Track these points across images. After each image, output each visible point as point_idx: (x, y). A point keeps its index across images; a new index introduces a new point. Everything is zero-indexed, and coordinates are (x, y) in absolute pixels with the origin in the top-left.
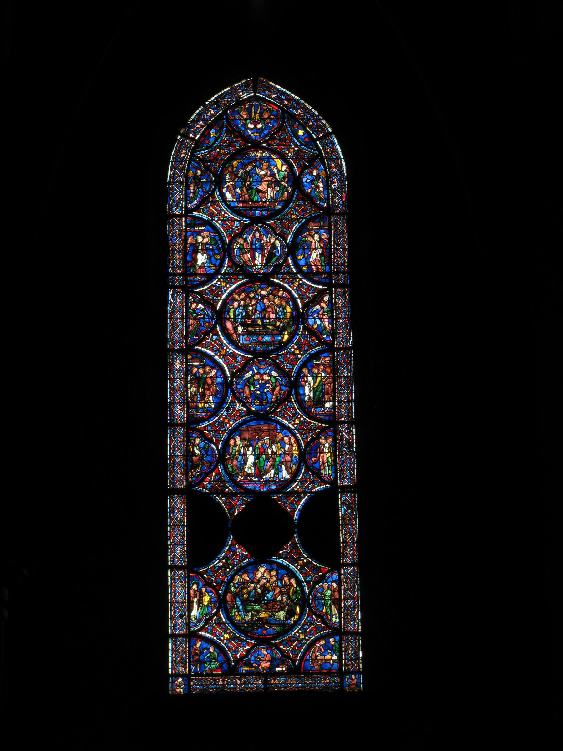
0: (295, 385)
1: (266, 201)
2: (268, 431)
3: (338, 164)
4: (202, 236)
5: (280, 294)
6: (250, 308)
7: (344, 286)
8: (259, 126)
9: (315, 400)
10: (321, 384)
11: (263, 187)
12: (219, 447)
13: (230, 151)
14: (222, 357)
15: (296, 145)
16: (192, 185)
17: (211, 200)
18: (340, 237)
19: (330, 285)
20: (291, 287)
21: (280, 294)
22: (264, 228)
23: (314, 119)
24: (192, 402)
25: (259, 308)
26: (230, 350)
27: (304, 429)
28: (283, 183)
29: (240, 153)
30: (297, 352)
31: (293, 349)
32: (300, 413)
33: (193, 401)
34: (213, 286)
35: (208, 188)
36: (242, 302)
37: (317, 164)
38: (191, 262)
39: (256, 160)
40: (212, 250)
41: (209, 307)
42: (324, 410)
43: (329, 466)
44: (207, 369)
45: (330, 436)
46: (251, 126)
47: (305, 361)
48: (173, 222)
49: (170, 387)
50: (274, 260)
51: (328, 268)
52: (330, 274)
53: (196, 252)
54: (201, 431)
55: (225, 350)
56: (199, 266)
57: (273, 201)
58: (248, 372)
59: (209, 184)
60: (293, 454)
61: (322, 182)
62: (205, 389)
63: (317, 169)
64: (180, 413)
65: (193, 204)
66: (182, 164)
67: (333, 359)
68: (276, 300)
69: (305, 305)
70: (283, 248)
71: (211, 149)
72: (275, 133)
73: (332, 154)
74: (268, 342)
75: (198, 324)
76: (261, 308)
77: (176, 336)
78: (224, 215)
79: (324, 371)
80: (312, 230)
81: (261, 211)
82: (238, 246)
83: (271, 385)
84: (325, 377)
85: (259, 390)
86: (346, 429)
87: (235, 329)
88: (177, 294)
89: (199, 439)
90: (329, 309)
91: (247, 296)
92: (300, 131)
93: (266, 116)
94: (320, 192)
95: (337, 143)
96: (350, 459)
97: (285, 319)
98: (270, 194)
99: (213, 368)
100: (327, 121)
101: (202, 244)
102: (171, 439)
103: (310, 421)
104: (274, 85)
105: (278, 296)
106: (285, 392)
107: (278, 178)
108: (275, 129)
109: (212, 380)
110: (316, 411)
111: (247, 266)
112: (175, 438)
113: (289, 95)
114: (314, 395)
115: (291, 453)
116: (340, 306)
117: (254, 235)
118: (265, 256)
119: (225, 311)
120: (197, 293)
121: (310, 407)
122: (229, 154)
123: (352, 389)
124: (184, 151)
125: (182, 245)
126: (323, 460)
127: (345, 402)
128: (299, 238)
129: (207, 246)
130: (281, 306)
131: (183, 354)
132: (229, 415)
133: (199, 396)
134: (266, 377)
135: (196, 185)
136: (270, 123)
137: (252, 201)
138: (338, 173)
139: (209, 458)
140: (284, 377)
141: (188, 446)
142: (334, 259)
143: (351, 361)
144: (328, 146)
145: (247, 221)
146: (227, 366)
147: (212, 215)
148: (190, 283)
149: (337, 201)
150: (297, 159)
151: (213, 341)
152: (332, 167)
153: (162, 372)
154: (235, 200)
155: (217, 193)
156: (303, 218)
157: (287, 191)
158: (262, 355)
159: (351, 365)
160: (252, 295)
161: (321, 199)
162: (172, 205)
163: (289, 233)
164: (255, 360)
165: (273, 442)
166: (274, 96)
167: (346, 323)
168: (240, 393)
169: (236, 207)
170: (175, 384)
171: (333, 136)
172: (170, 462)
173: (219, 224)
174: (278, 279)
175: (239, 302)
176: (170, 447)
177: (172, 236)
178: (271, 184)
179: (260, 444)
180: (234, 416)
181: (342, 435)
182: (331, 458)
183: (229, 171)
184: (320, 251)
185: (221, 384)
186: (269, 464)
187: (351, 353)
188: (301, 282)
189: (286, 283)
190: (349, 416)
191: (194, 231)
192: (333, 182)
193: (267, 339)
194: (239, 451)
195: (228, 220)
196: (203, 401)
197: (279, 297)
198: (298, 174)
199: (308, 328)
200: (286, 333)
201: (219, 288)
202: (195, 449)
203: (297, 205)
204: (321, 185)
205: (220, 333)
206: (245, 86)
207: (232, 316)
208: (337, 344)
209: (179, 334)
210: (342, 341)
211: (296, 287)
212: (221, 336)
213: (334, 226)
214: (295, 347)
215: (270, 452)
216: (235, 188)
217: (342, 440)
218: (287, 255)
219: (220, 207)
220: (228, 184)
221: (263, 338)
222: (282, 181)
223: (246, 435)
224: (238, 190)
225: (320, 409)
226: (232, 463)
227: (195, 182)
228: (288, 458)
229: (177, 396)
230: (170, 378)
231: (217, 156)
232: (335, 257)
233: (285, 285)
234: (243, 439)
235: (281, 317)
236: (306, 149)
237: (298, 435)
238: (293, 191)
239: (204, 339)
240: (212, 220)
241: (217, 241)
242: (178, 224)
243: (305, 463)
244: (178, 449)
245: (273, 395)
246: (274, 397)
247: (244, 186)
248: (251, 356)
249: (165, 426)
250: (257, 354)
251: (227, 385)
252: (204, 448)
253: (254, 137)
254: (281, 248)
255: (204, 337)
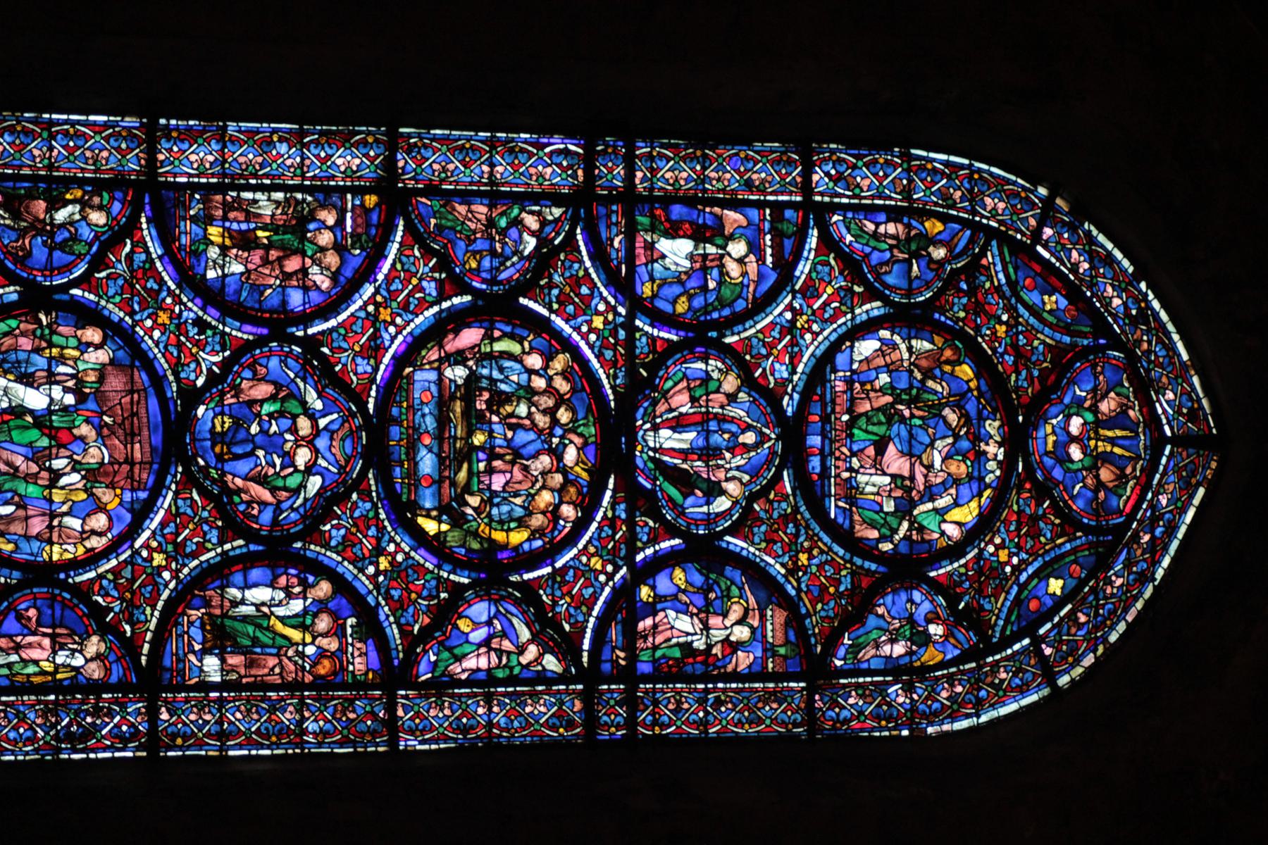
0: (278, 553)
1: (851, 470)
2: (126, 461)
3: (960, 706)
4: (746, 256)
5: (568, 511)
6: (522, 410)
7: (591, 720)
8: (1075, 452)
9: (228, 622)
10: (279, 641)
11: (895, 461)
12: (76, 292)
13: (1002, 355)
14: (371, 308)
15: (1017, 570)
16: (900, 227)
17: (857, 289)
18: (741, 712)
19: (591, 677)
20: (585, 547)
21: (568, 511)
22: (768, 462)
23: (1096, 628)
24: (224, 203)
25: (522, 437)
26: (393, 339)
27: (134, 580)
28: (905, 525)
29: (996, 390)
30: (384, 563)
31: (392, 548)
32: (186, 571)
33: (227, 207)
34: (593, 286)
35: (890, 280)
36: (539, 383)
37: (960, 636)
38: (668, 219)
39: (977, 437)
40: (704, 289)
41: (528, 270)
42: (194, 652)
43: (9, 666)
44: (332, 259)
45: (108, 671)
46: (1075, 425)
47: (355, 590)
48: (790, 162)
49: (275, 131)
50: (673, 492)
51: (645, 668)
52: (628, 675)
53: (699, 234)
54: (129, 229)
55: (393, 323)
56: (653, 243)
57: (851, 493)
58: (320, 397)
59: (904, 284)
60: (51, 543)
61: (910, 653)
62: (267, 248)
63: (946, 636)
64: (191, 160)
65: (844, 231)
66: (962, 199)
67: (360, 685)
68: (546, 498)
69: (529, 590)
70: (710, 520)
71: (1008, 293)
72: (1054, 504)
73: (992, 685)
74: (416, 464)
75: (474, 232)
76: (524, 446)
77: (437, 158)
78: (809, 330)
79: (322, 653)
80: (763, 618)
81: (822, 450)
82: (715, 375)
83: (277, 474)
84: (302, 655)
85: (264, 432)
86: (131, 725)
87: (459, 358)
88: (570, 167)
89: (102, 221)
90: (517, 670)
91: (560, 400)
92: (1060, 582)
93: (1106, 474)
94: (877, 647)
95: (1024, 702)
96: (32, 740)
97: (489, 524)
98: (871, 482)
99: (335, 277)
100: (1089, 670)
101: (722, 256)
102: (106, 126)
103: (160, 605)
104: (1196, 501)
105: (561, 502)
106: (256, 519)
107: (922, 508)
108: (1065, 502)
109: (296, 272)
110: (191, 623)
111: (655, 403)
112: (107, 139)
113: (1165, 549)
114: (245, 619)
115: (55, 539)
116: (528, 709)
117: (749, 428)
118: (685, 461)
119: (514, 326)
120: (571, 236)
121: (207, 603)
122: (994, 350)
123: (262, 747)
124: (1001, 205)
125: (719, 191)
126: (30, 645)
127: (220, 722)
128: (737, 575)
129: (715, 272)
130: (529, 513)
131: (379, 180)
132: (181, 328)
133: (244, 226)
134: (303, 457)
135: (900, 244)
136: (1085, 486)
137: (851, 424)
138: (936, 705)
139: (40, 254)
140: (304, 518)
141: (81, 183)
142: (674, 690)
143: (354, 744)
144: (1015, 675)
145: (789, 405)
146: (340, 325)
147: (810, 291)
148: (602, 210)
149: (851, 701)
150: (980, 572)
151: (420, 279)
152: (952, 686)
153: (321, 107)
154: (855, 366)
155: (874, 308)
156: (799, 590)
157: (883, 538)
158: (377, 442)
159: (341, 744)
160: (564, 416)
161: (856, 648)
162: (840, 160)
163: (753, 544)
164: (358, 421)
165: (93, 475)
166: (1164, 502)
167: (472, 728)
168: (252, 367)
169: (835, 371)
170: (283, 148)
171: (1046, 692)
172: (29, 120)
173: (781, 314)
174: (614, 505)
175: (543, 372)
176: (79, 123)
177: (747, 158)
178: (902, 487)
179: (85, 430)
180: (180, 345)
181: (111, 714)
182: (35, 674)
183: (941, 350)
184: (699, 644)
185: (284, 302)
186: (19, 461)
187: (377, 745)
188: (602, 578)
189: (600, 528)
190: (174, 736)
191: (761, 231)
192: (909, 689)
193: (427, 463)
194: (62, 360)
195: (793, 343)
196: (228, 242)
197: (557, 507)
198: (933, 574)
199: (457, 598)
200: (444, 527)
201: (585, 306)
202: (70, 208)
203: (838, 569)
204: (899, 649)
205: (445, 305)
206: (1191, 409)
207: (498, 347)
208: (406, 697)
209: (444, 170)
210: (418, 714)
211: (587, 565)
212: (436, 309)
213: (774, 693)
214: (400, 558)
215: (58, 464)
216: (890, 369)
217: (97, 712)
218: (685, 535)
219: (833, 320)
220: (903, 347)
221: (430, 451)
222: (911, 523)
223: (115, 383)
224: (884, 378)
225: (199, 638)
226: (23, 334)
227: (909, 239)
228: (37, 525)
229: (245, 155)
230: (302, 134)
231: (986, 313)
232: (678, 692)
233: (594, 525)
234: (102, 372)
235: (495, 511)
236: (1004, 602)
237: (114, 562)
238: (881, 558)
239: (428, 253)
240: (794, 292)
241: (731, 304)
242: (783, 179)
243: (21, 585)
244: (71, 151)
245: (246, 478)
246: (239, 482)
247: (898, 400)
248: (371, 406)
249: (149, 110)
250: (378, 426)
251: (279, 324)
252: (75, 238)
253: (1041, 434)
254: (709, 514)
255: (434, 253)
